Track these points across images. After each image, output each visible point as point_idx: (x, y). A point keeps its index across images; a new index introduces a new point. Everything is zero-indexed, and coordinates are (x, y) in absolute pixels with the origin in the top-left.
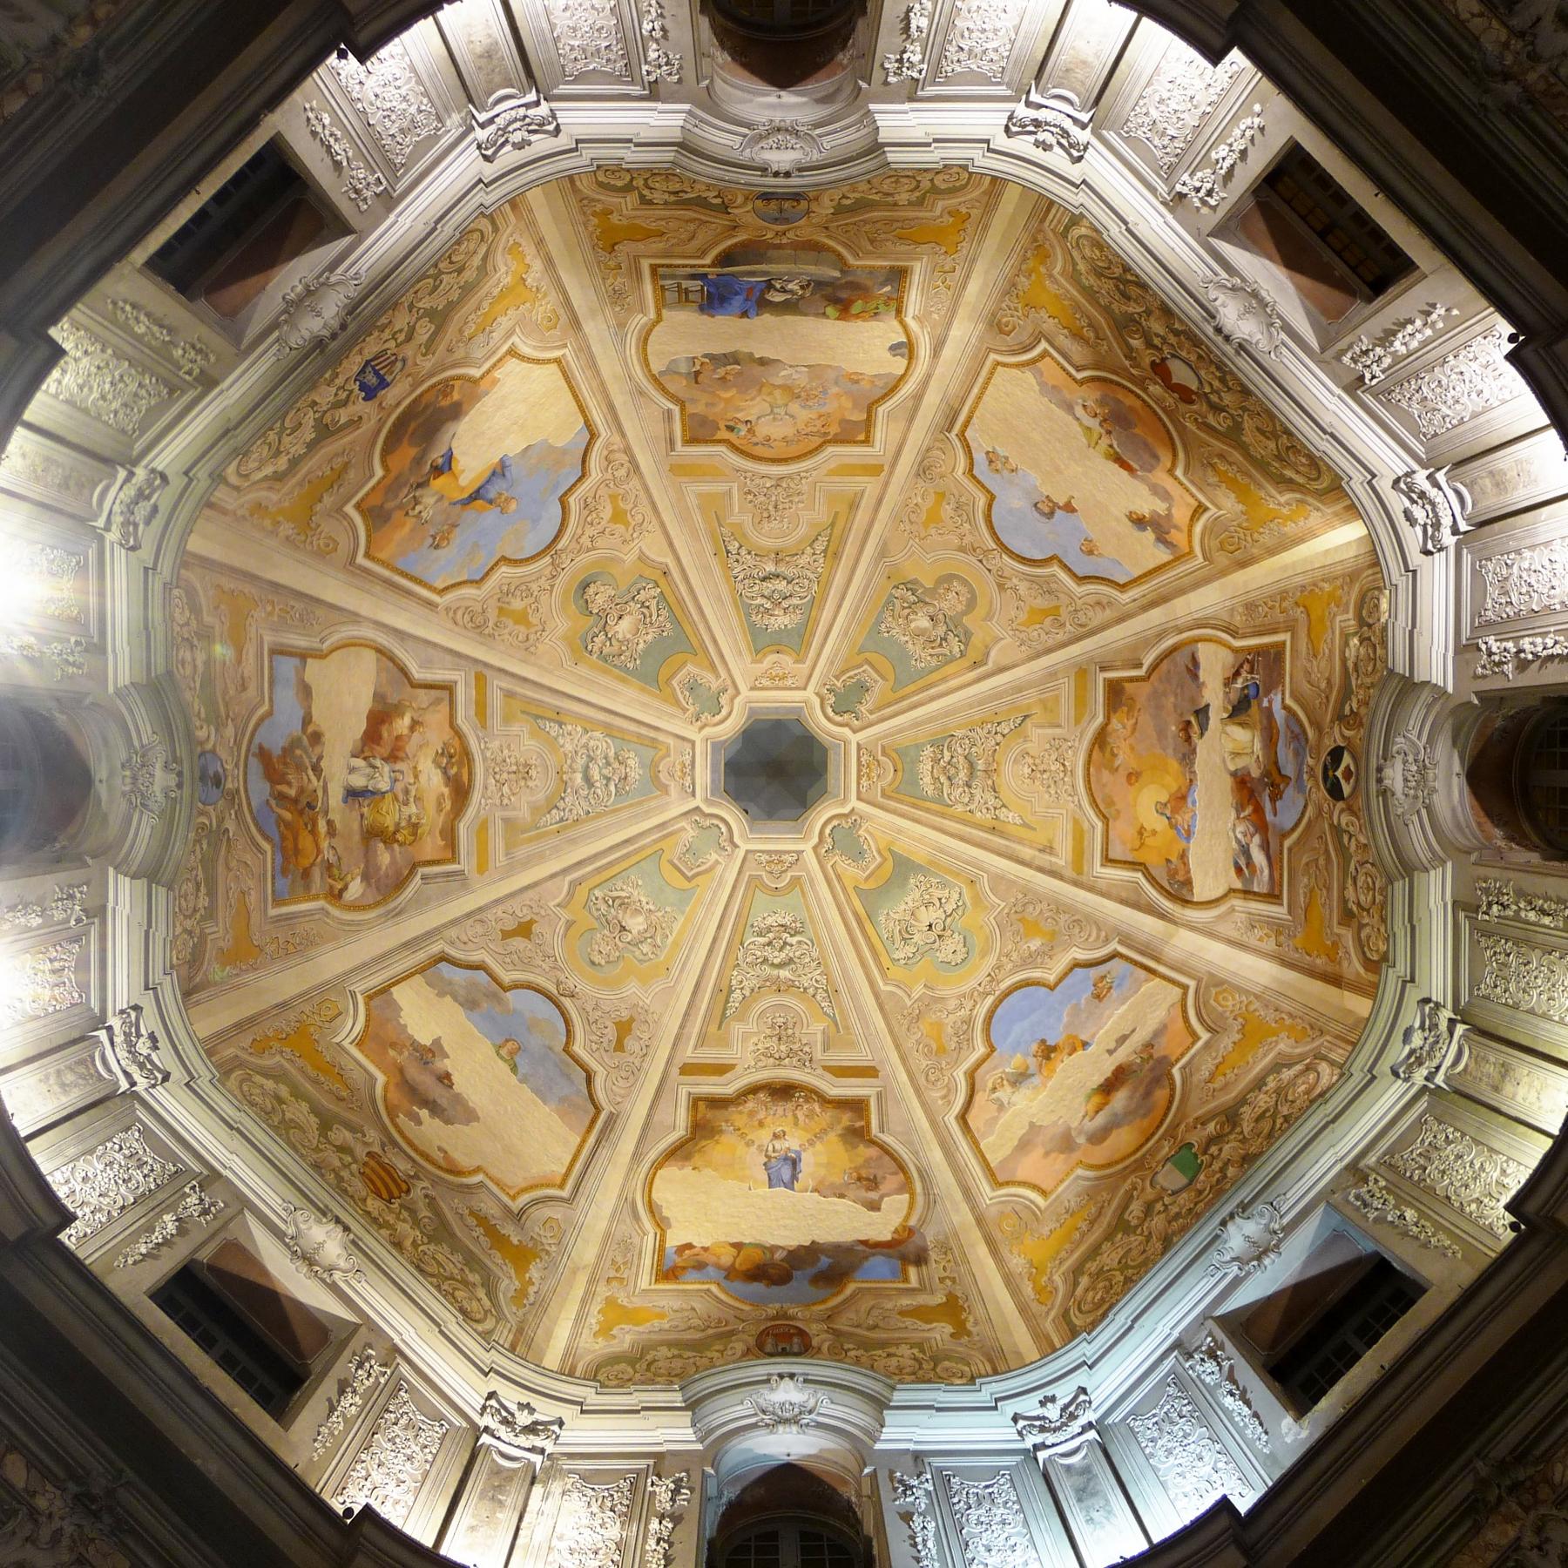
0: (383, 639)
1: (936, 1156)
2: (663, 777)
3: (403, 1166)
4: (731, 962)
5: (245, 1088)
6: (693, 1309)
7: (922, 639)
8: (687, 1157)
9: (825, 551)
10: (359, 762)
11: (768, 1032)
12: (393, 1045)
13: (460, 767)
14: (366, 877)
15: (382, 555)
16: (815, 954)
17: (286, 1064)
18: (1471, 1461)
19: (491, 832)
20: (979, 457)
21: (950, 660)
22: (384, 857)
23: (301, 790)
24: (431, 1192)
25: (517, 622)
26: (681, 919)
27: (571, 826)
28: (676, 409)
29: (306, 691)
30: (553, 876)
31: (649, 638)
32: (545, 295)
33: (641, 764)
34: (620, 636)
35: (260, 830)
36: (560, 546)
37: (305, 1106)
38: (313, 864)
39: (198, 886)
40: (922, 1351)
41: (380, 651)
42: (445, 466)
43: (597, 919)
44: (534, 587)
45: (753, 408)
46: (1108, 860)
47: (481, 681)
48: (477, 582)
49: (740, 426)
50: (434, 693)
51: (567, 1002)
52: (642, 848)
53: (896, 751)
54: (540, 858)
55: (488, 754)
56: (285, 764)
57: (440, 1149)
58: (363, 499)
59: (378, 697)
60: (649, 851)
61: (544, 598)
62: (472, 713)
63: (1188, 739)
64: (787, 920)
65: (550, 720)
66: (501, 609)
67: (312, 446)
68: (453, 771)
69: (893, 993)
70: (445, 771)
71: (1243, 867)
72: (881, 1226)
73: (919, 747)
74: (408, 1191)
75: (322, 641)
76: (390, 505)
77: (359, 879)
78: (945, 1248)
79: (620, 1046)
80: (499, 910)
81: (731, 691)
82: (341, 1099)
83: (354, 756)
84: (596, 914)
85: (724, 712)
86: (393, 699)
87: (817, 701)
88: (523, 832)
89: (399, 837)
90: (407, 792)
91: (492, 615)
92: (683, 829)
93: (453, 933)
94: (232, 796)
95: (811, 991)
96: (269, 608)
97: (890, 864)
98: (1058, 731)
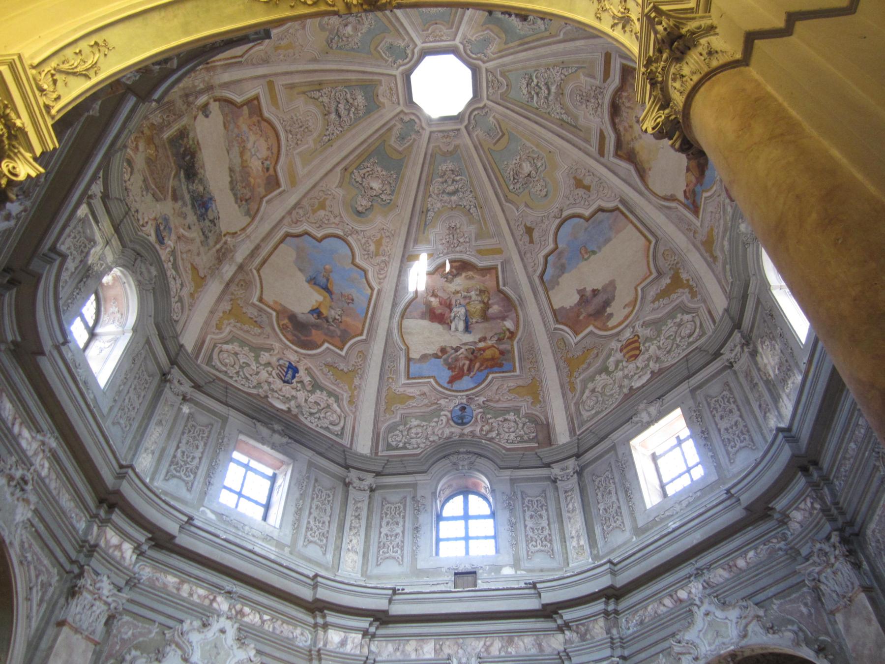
2: (451, 148)
3: (628, 334)
4: (547, 116)
5: (587, 408)
6: (712, 212)
7: (358, 26)
8: (644, 171)
9: (319, 91)
10: (453, 326)
12: (578, 315)
14: (504, 318)
15: (360, 326)
16: (543, 70)
17: (581, 378)
19: (482, 248)
22: (495, 309)
23: (466, 358)
24: (641, 322)
28: (265, 200)
29: (424, 357)
30: (503, 211)
31: (379, 169)
32: (232, 294)
33: (445, 161)
34: (381, 186)
37: (598, 377)
38: (498, 349)
39: (506, 420)
41: (403, 316)
42: (316, 312)
44: (363, 241)
45: (255, 165)
48: (365, 272)
49: (265, 165)
51: (565, 214)
55: (445, 251)
56: (455, 368)
58: (338, 348)
59: (423, 317)
60: (489, 156)
64: (524, 82)
66: (377, 255)
67: (322, 389)
69: (564, 34)
74: (638, 336)
75: (401, 350)
76: (339, 333)
79: (588, 188)
80: (520, 243)
81: (402, 116)
84: (521, 190)
85: (413, 117)
86: (423, 308)
87: (402, 68)
89: (486, 300)
90: (465, 297)
91: (379, 259)
92: (477, 135)
93: (530, 269)
94: (469, 399)
95: (563, 77)
96: (391, 380)
97: (490, 26)
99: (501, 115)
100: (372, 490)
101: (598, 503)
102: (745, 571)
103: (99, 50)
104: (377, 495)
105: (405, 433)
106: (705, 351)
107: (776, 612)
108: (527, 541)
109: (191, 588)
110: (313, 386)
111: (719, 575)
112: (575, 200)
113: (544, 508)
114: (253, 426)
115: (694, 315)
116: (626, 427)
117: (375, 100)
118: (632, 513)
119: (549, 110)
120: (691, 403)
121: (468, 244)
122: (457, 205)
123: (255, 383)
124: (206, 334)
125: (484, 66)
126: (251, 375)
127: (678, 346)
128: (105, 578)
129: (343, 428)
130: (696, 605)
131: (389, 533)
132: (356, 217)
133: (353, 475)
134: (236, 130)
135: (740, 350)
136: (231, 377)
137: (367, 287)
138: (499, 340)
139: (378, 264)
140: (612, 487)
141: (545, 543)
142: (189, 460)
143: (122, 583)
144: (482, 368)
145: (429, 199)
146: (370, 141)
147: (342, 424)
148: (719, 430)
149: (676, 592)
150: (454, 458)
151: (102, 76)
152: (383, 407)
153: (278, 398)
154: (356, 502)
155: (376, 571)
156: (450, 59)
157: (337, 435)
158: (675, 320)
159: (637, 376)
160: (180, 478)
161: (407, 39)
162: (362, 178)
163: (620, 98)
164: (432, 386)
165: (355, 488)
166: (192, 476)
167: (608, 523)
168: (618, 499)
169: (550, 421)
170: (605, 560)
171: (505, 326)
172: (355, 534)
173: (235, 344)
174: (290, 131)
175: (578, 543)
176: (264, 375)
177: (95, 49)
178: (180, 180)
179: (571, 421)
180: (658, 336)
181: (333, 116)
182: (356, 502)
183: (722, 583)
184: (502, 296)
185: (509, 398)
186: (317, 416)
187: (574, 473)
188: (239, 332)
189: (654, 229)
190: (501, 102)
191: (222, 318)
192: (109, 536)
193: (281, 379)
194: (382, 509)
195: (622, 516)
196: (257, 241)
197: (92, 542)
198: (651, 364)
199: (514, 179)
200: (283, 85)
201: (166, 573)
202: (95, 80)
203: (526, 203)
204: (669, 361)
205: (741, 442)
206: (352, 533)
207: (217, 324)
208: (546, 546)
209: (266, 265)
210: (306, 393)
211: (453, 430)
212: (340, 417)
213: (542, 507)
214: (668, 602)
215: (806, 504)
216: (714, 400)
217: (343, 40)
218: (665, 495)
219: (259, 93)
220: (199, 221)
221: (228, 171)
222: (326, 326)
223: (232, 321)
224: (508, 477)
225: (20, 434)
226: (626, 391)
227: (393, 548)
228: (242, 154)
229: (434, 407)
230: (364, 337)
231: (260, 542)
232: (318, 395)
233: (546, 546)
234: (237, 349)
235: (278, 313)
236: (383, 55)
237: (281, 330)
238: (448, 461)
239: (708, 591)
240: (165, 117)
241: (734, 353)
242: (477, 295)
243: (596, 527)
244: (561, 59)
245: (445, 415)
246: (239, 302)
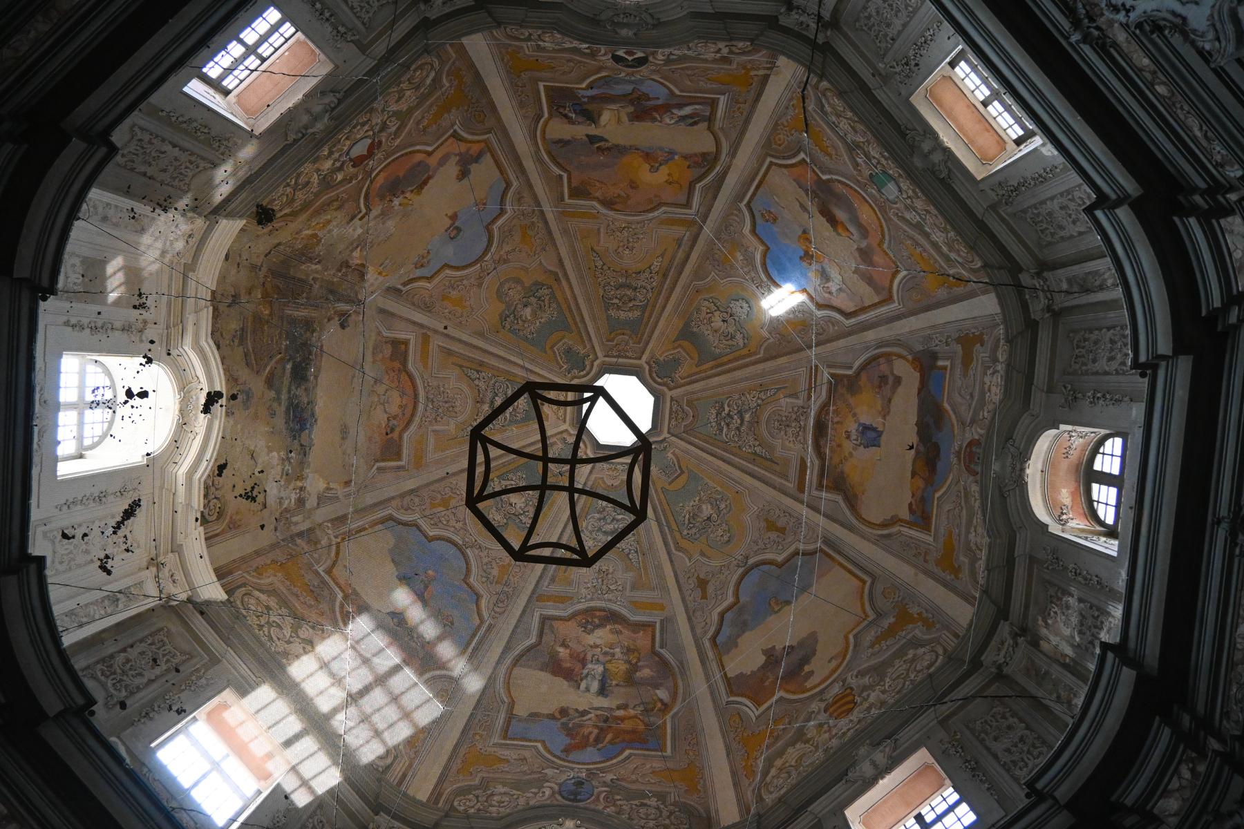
0: (508, 661)
1: (871, 335)
3: (836, 689)
8: (855, 496)
9: (478, 372)
10: (583, 685)
11: (783, 433)
14: (656, 686)
16: (737, 396)
18: (1071, 44)
20: (418, 273)
21: (553, 296)
27: (641, 547)
29: (534, 716)
30: (671, 561)
34: (523, 505)
35: (615, 757)
36: (460, 542)
37: (790, 750)
39: (643, 805)
40: (989, 368)
41: (516, 662)
44: (485, 560)
46: (688, 205)
48: (478, 597)
51: (751, 561)
52: (659, 500)
54: (659, 567)
57: (829, 661)
60: (662, 496)
62: (561, 605)
63: (609, 149)
64: (714, 412)
68: (596, 621)
70: (598, 627)
71: (693, 120)
72: (910, 378)
73: (609, 318)
74: (852, 689)
75: (503, 702)
77: (657, 691)
78: (929, 338)
79: (782, 530)
81: (565, 435)
90: (606, 654)
91: (499, 588)
93: (699, 631)
95: (759, 401)
96: (477, 737)
97: (685, 344)
98: (602, 230)
116: (838, 789)
124: (238, 568)
125: (669, 394)
126: (279, 639)
135: (1011, 642)
137: (476, 616)
138: (646, 710)
144: (617, 740)
158: (905, 658)
161: (588, 346)
163: (827, 413)
169: (713, 814)
171: (656, 695)
180: (882, 680)
184: (657, 659)
185: (653, 781)
191: (266, 565)
199: (690, 523)
200: (439, 346)
215: (1180, 777)
241: (1002, 653)
245: (551, 788)
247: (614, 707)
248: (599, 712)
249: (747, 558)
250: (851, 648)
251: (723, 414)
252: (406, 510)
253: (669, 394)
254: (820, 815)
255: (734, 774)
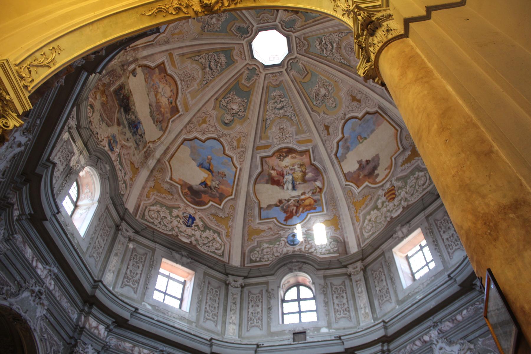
2: (278, 83)
3: (388, 186)
4: (332, 61)
5: (367, 231)
7: (219, 18)
9: (199, 56)
10: (285, 187)
12: (359, 176)
13: (282, 152)
14: (315, 180)
15: (231, 190)
16: (328, 35)
17: (363, 213)
19: (300, 139)
22: (310, 175)
24: (395, 178)
25: (240, 142)
26: (320, 76)
28: (171, 120)
29: (269, 207)
31: (236, 98)
32: (155, 177)
33: (275, 90)
34: (238, 107)
36: (216, 137)
37: (372, 212)
38: (313, 199)
41: (255, 183)
43: (322, 104)
44: (229, 140)
45: (164, 101)
47: (259, 148)
48: (231, 158)
49: (170, 100)
50: (264, 164)
51: (347, 117)
52: (300, 88)
53: (257, 14)
54: (306, 121)
55: (278, 143)
56: (288, 212)
57: (385, 170)
59: (267, 182)
60: (301, 86)
61: (232, 136)
62: (267, 150)
64: (318, 42)
65: (266, 123)
66: (238, 148)
67: (210, 229)
68: (284, 154)
70: (285, 157)
74: (394, 186)
75: (255, 203)
76: (218, 195)
79: (359, 101)
80: (322, 135)
81: (248, 66)
82: (371, 199)
83: (284, 189)
84: (321, 104)
85: (255, 66)
86: (267, 177)
87: (246, 40)
88: (299, 128)
89: (304, 170)
90: (291, 169)
91: (239, 150)
92: (293, 74)
93: (329, 151)
95: (340, 38)
96: (250, 221)
99: (306, 62)
100: (242, 287)
101: (376, 287)
102: (461, 322)
103: (55, 51)
104: (246, 290)
105: (260, 252)
106: (432, 193)
107: (481, 346)
108: (335, 312)
109: (139, 349)
110: (204, 228)
111: (447, 326)
112: (352, 108)
113: (344, 292)
114: (170, 253)
115: (425, 172)
116: (390, 240)
117: (232, 58)
118: (395, 292)
119: (333, 57)
120: (426, 224)
121: (291, 138)
122: (284, 115)
123: (170, 228)
124: (141, 201)
126: (168, 223)
127: (417, 191)
128: (90, 346)
129: (223, 252)
130: (434, 344)
131: (254, 312)
132: (224, 126)
133: (230, 279)
134: (152, 83)
136: (156, 226)
137: (233, 167)
138: (313, 193)
139: (239, 153)
140: (383, 277)
141: (345, 312)
142: (134, 275)
143: (100, 349)
144: (304, 211)
145: (267, 113)
146: (231, 81)
147: (223, 249)
148: (443, 240)
149: (423, 337)
150: (290, 266)
151: (57, 65)
152: (246, 238)
153: (184, 236)
154: (233, 294)
155: (247, 334)
156: (274, 32)
157: (220, 256)
158: (415, 176)
159: (394, 210)
160: (129, 286)
161: (248, 23)
162: (227, 103)
164: (275, 223)
165: (232, 286)
166: (137, 284)
167: (382, 298)
168: (387, 284)
169: (346, 239)
170: (380, 321)
172: (234, 314)
173: (158, 205)
174: (183, 80)
175: (365, 312)
176: (175, 223)
177: (53, 51)
178: (121, 113)
179: (358, 239)
180: (406, 186)
181: (208, 69)
182: (233, 294)
183: (449, 330)
184: (313, 167)
186: (207, 245)
187: (361, 270)
188: (160, 199)
189: (399, 123)
190: (305, 54)
191: (149, 191)
192: (91, 322)
193: (185, 224)
194: (249, 298)
195: (389, 294)
196: (167, 145)
197: (81, 326)
198: (403, 202)
199: (316, 98)
200: (178, 55)
201: (125, 341)
202: (53, 68)
203: (324, 112)
204: (413, 200)
205: (456, 246)
206: (232, 313)
207: (147, 195)
208: (346, 314)
209: (173, 158)
210: (200, 231)
211: (288, 249)
212: (221, 245)
213: (343, 291)
214: (418, 343)
216: (439, 222)
217: (211, 27)
218: (414, 279)
219: (164, 60)
220: (133, 136)
221: (148, 106)
222: (210, 192)
223: (155, 192)
224: (322, 275)
225: (37, 266)
226: (388, 219)
227: (256, 320)
228: (156, 96)
229: (277, 236)
230: (233, 197)
231: (178, 321)
232: (208, 233)
233: (346, 314)
234: (159, 209)
235: (182, 186)
236: (235, 33)
237: (184, 196)
238: (286, 267)
239: (441, 335)
240: (111, 79)
242: (298, 167)
243: (375, 301)
244: (337, 28)
245: (284, 240)
246: (159, 181)
247: (300, 194)
248: (294, 199)
249: (345, 115)
250: (393, 165)
251: (323, 44)
252: (189, 133)
253: (294, 35)
254: (384, 250)
255: (352, 219)
